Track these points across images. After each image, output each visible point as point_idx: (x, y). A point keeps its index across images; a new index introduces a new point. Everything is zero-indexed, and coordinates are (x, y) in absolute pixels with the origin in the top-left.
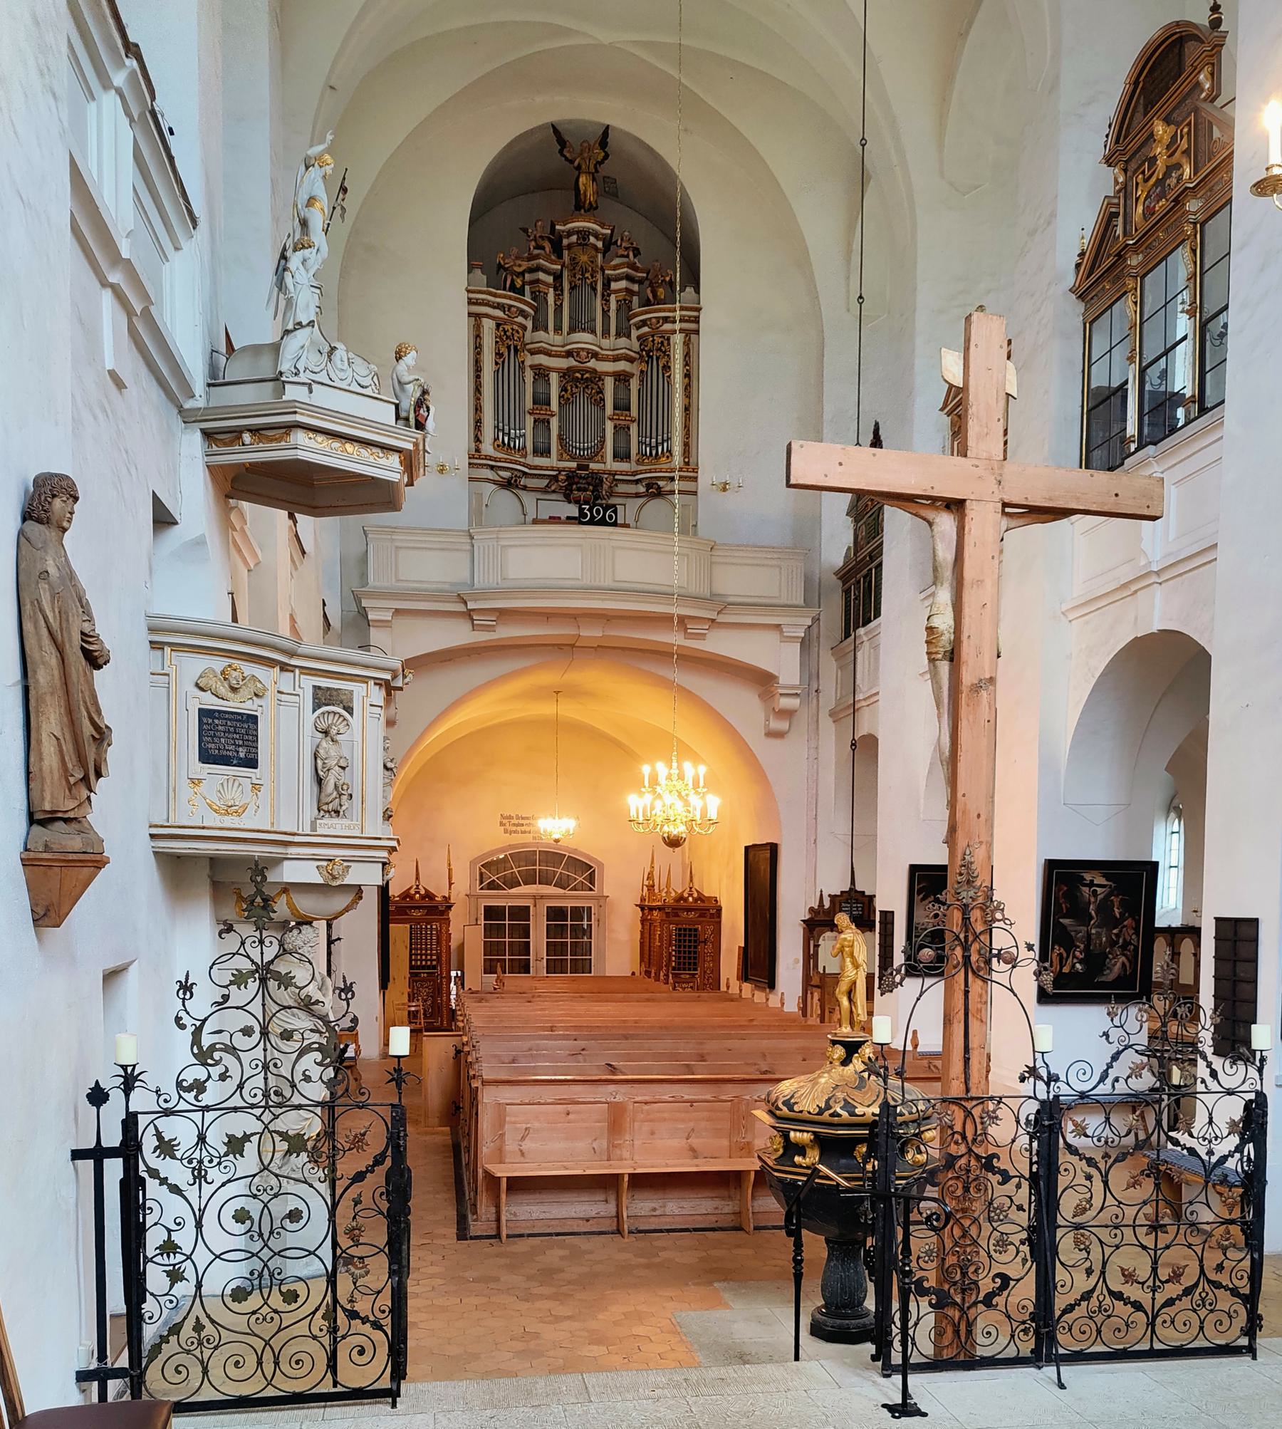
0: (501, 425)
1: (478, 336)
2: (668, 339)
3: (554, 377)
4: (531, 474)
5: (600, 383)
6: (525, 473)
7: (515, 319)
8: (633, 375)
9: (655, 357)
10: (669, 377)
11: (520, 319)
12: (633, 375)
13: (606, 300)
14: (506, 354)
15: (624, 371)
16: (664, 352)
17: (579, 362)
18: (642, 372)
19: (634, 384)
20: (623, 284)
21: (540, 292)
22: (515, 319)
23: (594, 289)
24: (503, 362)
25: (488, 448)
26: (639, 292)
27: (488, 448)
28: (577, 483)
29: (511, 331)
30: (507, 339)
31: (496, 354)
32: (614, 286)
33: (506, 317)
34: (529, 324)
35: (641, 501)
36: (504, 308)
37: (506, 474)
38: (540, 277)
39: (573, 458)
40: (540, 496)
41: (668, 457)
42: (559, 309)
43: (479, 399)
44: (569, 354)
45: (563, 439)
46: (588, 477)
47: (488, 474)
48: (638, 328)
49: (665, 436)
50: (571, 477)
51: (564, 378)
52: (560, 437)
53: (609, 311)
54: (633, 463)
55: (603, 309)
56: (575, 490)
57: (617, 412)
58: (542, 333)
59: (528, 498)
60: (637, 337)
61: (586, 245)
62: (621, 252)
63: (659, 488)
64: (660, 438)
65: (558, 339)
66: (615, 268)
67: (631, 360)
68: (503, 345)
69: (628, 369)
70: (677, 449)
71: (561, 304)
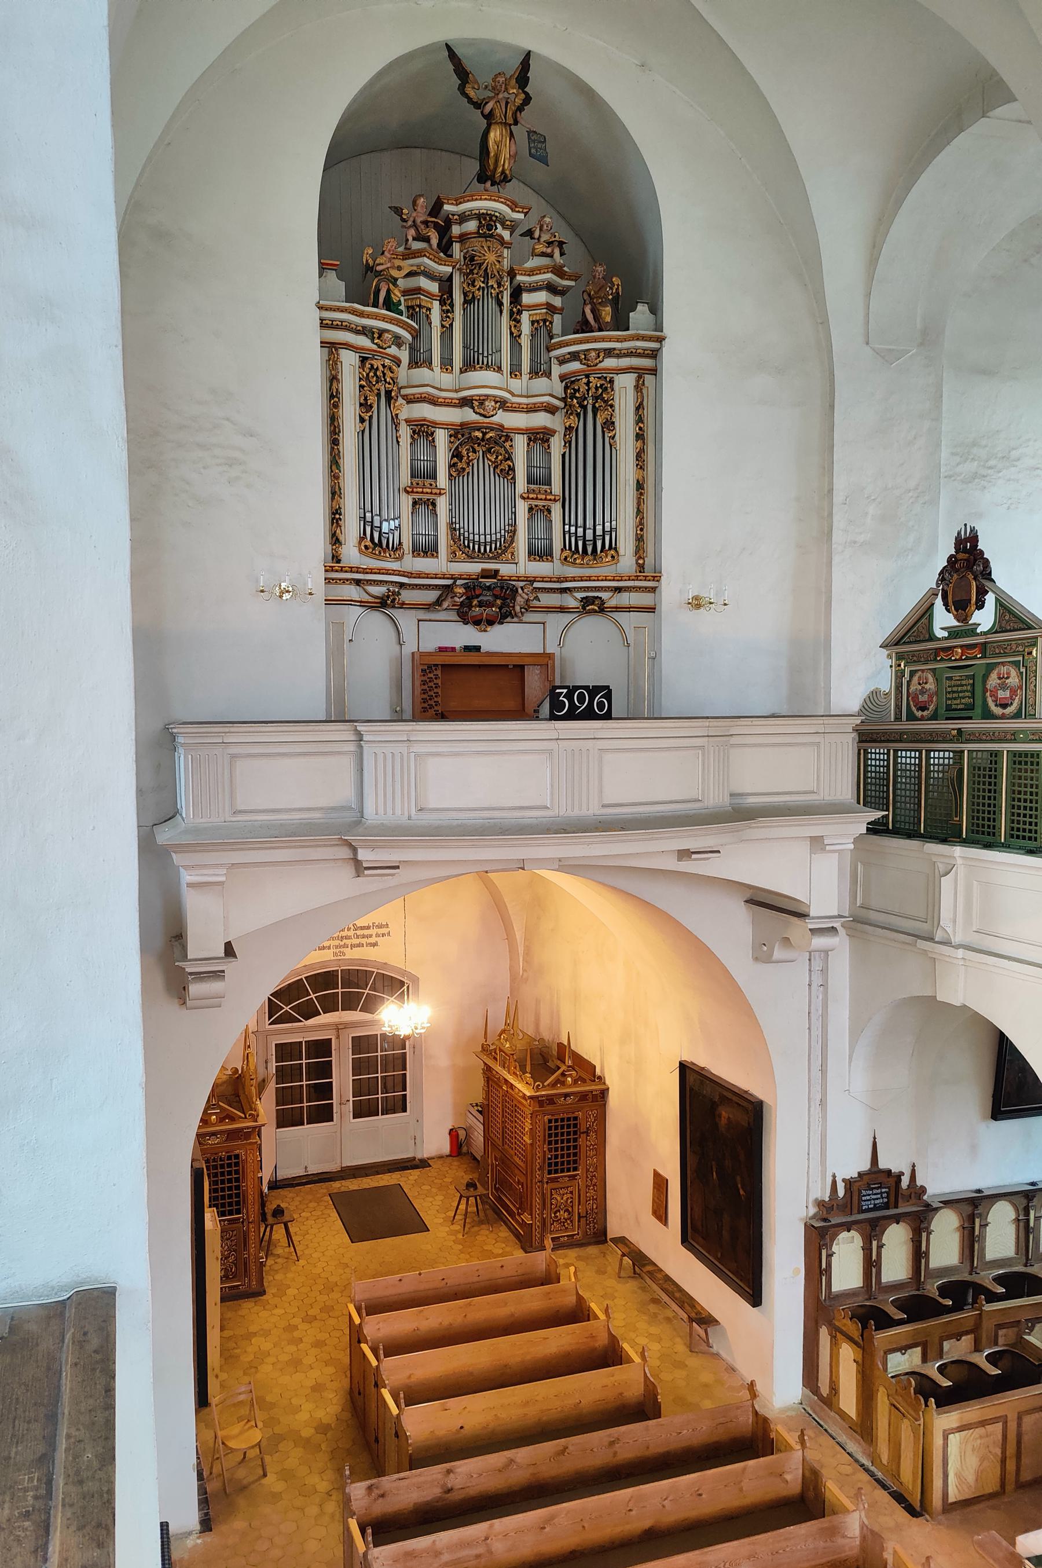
0: (368, 515)
1: (333, 378)
2: (611, 381)
3: (441, 437)
4: (410, 585)
5: (507, 445)
6: (402, 585)
7: (388, 351)
8: (555, 432)
9: (590, 408)
10: (613, 437)
11: (393, 350)
12: (551, 432)
13: (515, 318)
14: (375, 406)
15: (545, 428)
16: (606, 402)
17: (481, 415)
18: (569, 429)
19: (557, 445)
20: (542, 297)
21: (420, 306)
22: (388, 351)
23: (500, 304)
24: (371, 417)
25: (351, 553)
26: (562, 309)
27: (351, 553)
28: (478, 596)
29: (381, 368)
30: (377, 382)
31: (361, 405)
32: (527, 298)
33: (375, 347)
34: (404, 355)
35: (567, 618)
36: (373, 333)
37: (378, 590)
38: (422, 285)
39: (471, 557)
40: (422, 614)
41: (613, 557)
42: (447, 331)
43: (337, 477)
44: (465, 402)
45: (455, 529)
46: (494, 588)
47: (353, 592)
48: (562, 361)
49: (607, 525)
50: (473, 587)
51: (456, 437)
52: (452, 528)
53: (519, 336)
54: (557, 562)
55: (511, 333)
56: (476, 606)
57: (532, 486)
58: (425, 371)
59: (407, 620)
60: (560, 377)
61: (491, 236)
62: (541, 248)
63: (603, 602)
64: (599, 528)
65: (446, 380)
66: (531, 272)
67: (551, 410)
68: (371, 391)
69: (549, 425)
70: (626, 544)
71: (451, 325)
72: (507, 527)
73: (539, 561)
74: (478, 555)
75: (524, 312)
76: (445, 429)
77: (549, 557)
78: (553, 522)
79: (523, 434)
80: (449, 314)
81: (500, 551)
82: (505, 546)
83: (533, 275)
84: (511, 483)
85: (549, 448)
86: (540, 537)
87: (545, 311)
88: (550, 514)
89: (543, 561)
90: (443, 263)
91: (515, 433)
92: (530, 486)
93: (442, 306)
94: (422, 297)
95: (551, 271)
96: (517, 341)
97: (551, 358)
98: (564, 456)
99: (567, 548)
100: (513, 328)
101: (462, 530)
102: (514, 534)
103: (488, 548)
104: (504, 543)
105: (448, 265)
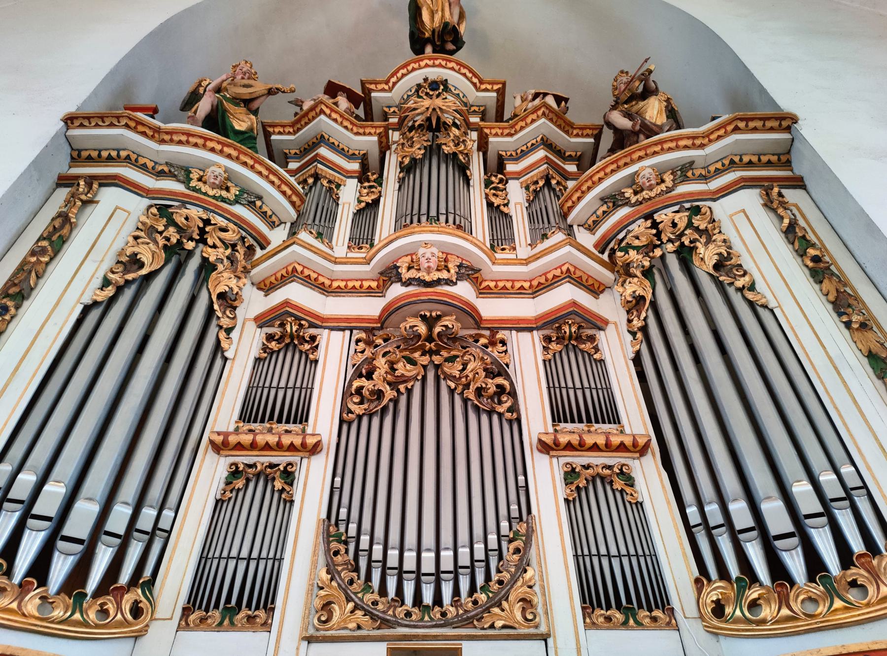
18: (636, 304)
21: (317, 177)
23: (463, 170)
53: (506, 205)
55: (490, 205)
72: (504, 524)
73: (625, 624)
74: (408, 614)
75: (509, 181)
76: (343, 330)
77: (657, 613)
78: (647, 506)
79: (530, 330)
80: (374, 190)
81: (482, 597)
82: (500, 582)
83: (516, 132)
84: (510, 422)
85: (597, 350)
86: (613, 551)
87: (546, 166)
88: (632, 486)
89: (639, 624)
90: (361, 131)
91: (510, 329)
92: (562, 425)
93: (362, 183)
94: (319, 166)
95: (544, 114)
96: (502, 212)
97: (571, 226)
98: (637, 360)
100: (493, 199)
101: (365, 539)
102: (528, 543)
103: (447, 590)
104: (499, 571)
105: (370, 134)
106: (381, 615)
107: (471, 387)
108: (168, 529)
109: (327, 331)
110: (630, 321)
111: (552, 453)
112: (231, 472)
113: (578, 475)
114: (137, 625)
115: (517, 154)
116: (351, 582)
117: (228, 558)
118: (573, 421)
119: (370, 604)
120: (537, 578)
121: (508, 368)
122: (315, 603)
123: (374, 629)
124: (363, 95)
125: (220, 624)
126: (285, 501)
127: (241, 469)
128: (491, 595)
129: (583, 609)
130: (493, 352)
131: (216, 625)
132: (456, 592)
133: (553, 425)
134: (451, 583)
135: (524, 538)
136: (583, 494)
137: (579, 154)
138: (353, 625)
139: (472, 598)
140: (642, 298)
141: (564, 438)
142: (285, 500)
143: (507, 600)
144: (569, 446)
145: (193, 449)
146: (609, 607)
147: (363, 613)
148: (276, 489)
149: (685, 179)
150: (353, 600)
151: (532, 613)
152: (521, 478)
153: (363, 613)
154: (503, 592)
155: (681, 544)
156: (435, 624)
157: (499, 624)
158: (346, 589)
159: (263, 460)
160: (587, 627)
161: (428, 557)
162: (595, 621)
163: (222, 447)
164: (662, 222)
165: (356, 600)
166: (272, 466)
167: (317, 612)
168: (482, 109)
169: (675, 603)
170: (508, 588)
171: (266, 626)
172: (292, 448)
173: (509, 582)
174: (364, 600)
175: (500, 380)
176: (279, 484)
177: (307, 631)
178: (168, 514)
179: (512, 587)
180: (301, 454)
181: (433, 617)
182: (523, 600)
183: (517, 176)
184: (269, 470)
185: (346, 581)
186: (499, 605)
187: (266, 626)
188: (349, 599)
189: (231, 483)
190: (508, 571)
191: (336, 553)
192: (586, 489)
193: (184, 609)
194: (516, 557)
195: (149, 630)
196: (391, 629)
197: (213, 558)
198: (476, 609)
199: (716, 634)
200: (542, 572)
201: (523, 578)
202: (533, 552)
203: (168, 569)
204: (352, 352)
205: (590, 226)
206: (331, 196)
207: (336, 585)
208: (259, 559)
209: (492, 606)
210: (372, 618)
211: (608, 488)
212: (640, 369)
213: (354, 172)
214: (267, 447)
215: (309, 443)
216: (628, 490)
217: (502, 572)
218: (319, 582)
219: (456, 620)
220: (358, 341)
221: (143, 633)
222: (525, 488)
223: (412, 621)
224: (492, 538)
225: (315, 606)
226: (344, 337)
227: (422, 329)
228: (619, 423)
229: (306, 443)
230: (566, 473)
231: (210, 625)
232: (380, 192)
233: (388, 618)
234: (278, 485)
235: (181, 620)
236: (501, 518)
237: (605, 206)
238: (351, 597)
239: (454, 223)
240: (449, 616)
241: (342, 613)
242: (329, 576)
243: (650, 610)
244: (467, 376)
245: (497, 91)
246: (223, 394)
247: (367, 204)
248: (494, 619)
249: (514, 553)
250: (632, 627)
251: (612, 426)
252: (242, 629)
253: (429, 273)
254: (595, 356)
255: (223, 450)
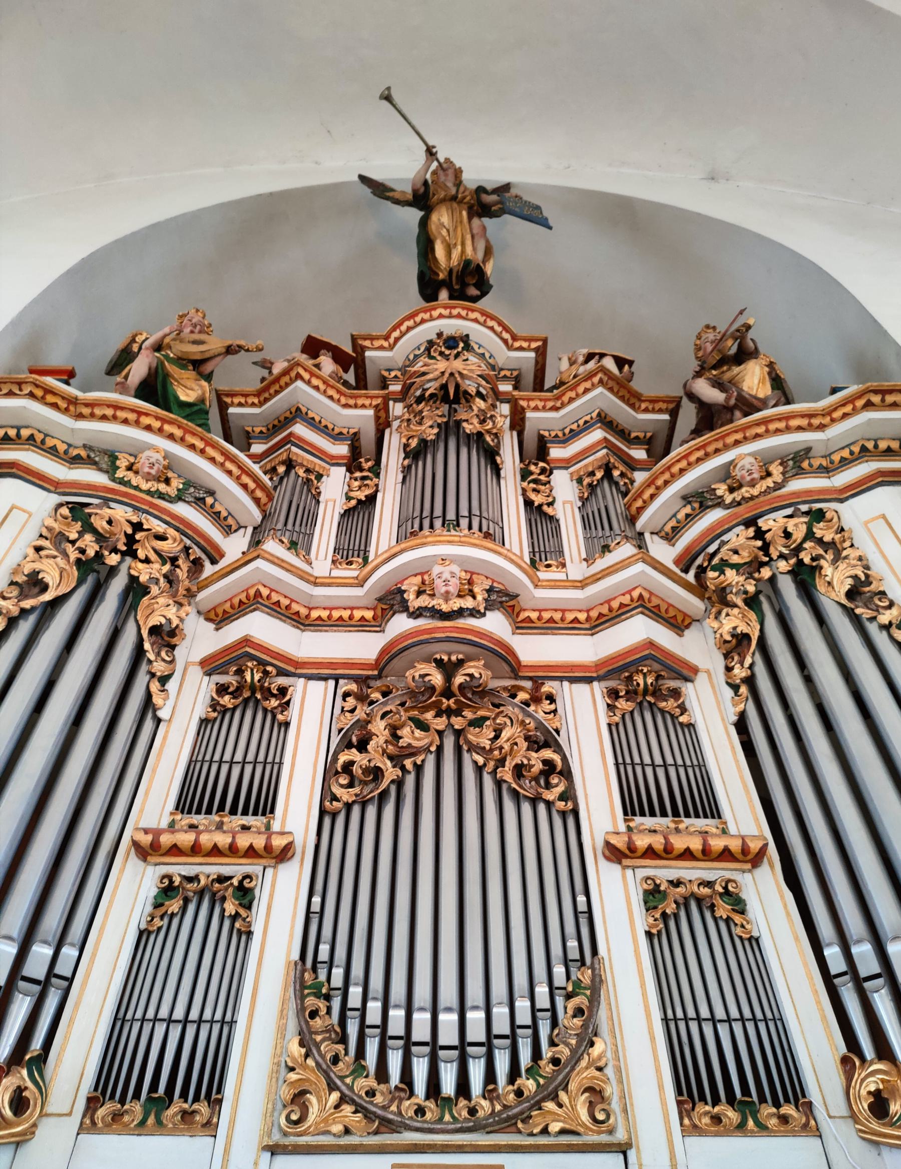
21: (290, 465)
23: (491, 455)
53: (550, 504)
55: (528, 503)
72: (559, 970)
73: (741, 1127)
74: (420, 1111)
75: (555, 471)
76: (325, 679)
77: (788, 1110)
78: (767, 944)
79: (589, 680)
81: (529, 1085)
82: (555, 1061)
83: (563, 405)
84: (563, 814)
85: (683, 709)
86: (720, 1014)
87: (605, 451)
88: (742, 912)
89: (762, 1128)
90: (352, 402)
91: (561, 679)
92: (638, 820)
93: (351, 472)
94: (294, 449)
95: (601, 381)
96: (546, 514)
97: (641, 534)
98: (741, 726)
99: (868, 1051)
100: (532, 496)
101: (355, 992)
102: (594, 1000)
103: (476, 1072)
104: (552, 1044)
105: (363, 406)
106: (379, 1112)
107: (507, 763)
108: (68, 974)
109: (302, 680)
110: (729, 669)
111: (626, 862)
112: (163, 888)
113: (664, 895)
114: (19, 1125)
115: (564, 434)
116: (336, 1060)
117: (155, 1020)
118: (653, 814)
119: (364, 1095)
120: (609, 1054)
121: (559, 735)
122: (282, 1093)
123: (369, 1133)
124: (354, 355)
125: (143, 1123)
126: (240, 933)
127: (176, 884)
128: (542, 1081)
129: (679, 1103)
130: (536, 712)
131: (135, 1126)
132: (490, 1076)
133: (626, 820)
134: (483, 1061)
135: (588, 992)
136: (672, 924)
137: (649, 435)
138: (337, 1128)
139: (513, 1085)
140: (746, 637)
141: (643, 840)
142: (239, 931)
143: (565, 1089)
144: (650, 853)
145: (109, 852)
146: (716, 1101)
147: (353, 1108)
148: (227, 914)
149: (800, 472)
150: (338, 1088)
151: (603, 1110)
152: (581, 899)
153: (353, 1108)
154: (560, 1077)
155: (818, 1002)
156: (461, 1128)
157: (555, 1127)
158: (329, 1070)
159: (209, 870)
160: (686, 1132)
161: (448, 1020)
162: (697, 1123)
163: (150, 852)
164: (769, 530)
165: (343, 1088)
166: (221, 879)
167: (285, 1106)
168: (515, 373)
169: (814, 1094)
170: (567, 1070)
171: (210, 1127)
172: (251, 852)
173: (568, 1061)
174: (355, 1088)
175: (548, 754)
176: (232, 906)
177: (269, 1136)
178: (69, 952)
179: (573, 1069)
180: (264, 862)
181: (456, 1115)
182: (589, 1089)
183: (566, 464)
184: (217, 885)
185: (328, 1058)
186: (555, 1097)
187: (210, 1127)
188: (332, 1087)
189: (162, 905)
190: (567, 1044)
191: (314, 1014)
192: (676, 916)
193: (90, 1100)
194: (578, 1022)
195: (36, 1133)
196: (395, 1135)
197: (133, 1019)
198: (520, 1103)
199: (876, 1144)
200: (617, 1046)
201: (589, 1054)
202: (602, 1014)
203: (66, 1038)
204: (337, 711)
205: (667, 534)
206: (309, 490)
207: (314, 1064)
208: (200, 1021)
209: (544, 1099)
210: (366, 1117)
211: (708, 915)
212: (745, 738)
213: (342, 457)
214: (215, 851)
215: (276, 846)
216: (737, 919)
217: (557, 1045)
218: (288, 1060)
219: (491, 1120)
220: (346, 695)
221: (27, 1137)
222: (587, 915)
223: (425, 1122)
224: (542, 990)
225: (282, 1097)
226: (326, 689)
227: (437, 679)
228: (720, 817)
229: (272, 846)
230: (647, 893)
231: (126, 1125)
232: (377, 485)
233: (391, 1116)
234: (230, 907)
235: (84, 1116)
236: (554, 961)
237: (689, 507)
238: (335, 1084)
239: (480, 530)
240: (481, 1114)
241: (322, 1109)
242: (303, 1051)
243: (777, 1105)
244: (501, 748)
245: (536, 350)
246: (154, 771)
247: (360, 502)
248: (549, 1118)
249: (574, 1016)
250: (752, 1131)
251: (709, 821)
252: (174, 1132)
253: (447, 600)
254: (681, 719)
255: (151, 855)
